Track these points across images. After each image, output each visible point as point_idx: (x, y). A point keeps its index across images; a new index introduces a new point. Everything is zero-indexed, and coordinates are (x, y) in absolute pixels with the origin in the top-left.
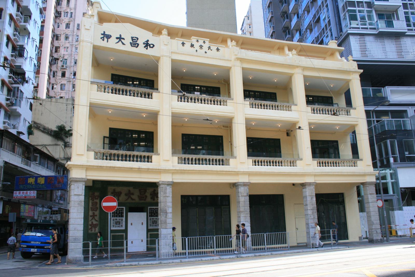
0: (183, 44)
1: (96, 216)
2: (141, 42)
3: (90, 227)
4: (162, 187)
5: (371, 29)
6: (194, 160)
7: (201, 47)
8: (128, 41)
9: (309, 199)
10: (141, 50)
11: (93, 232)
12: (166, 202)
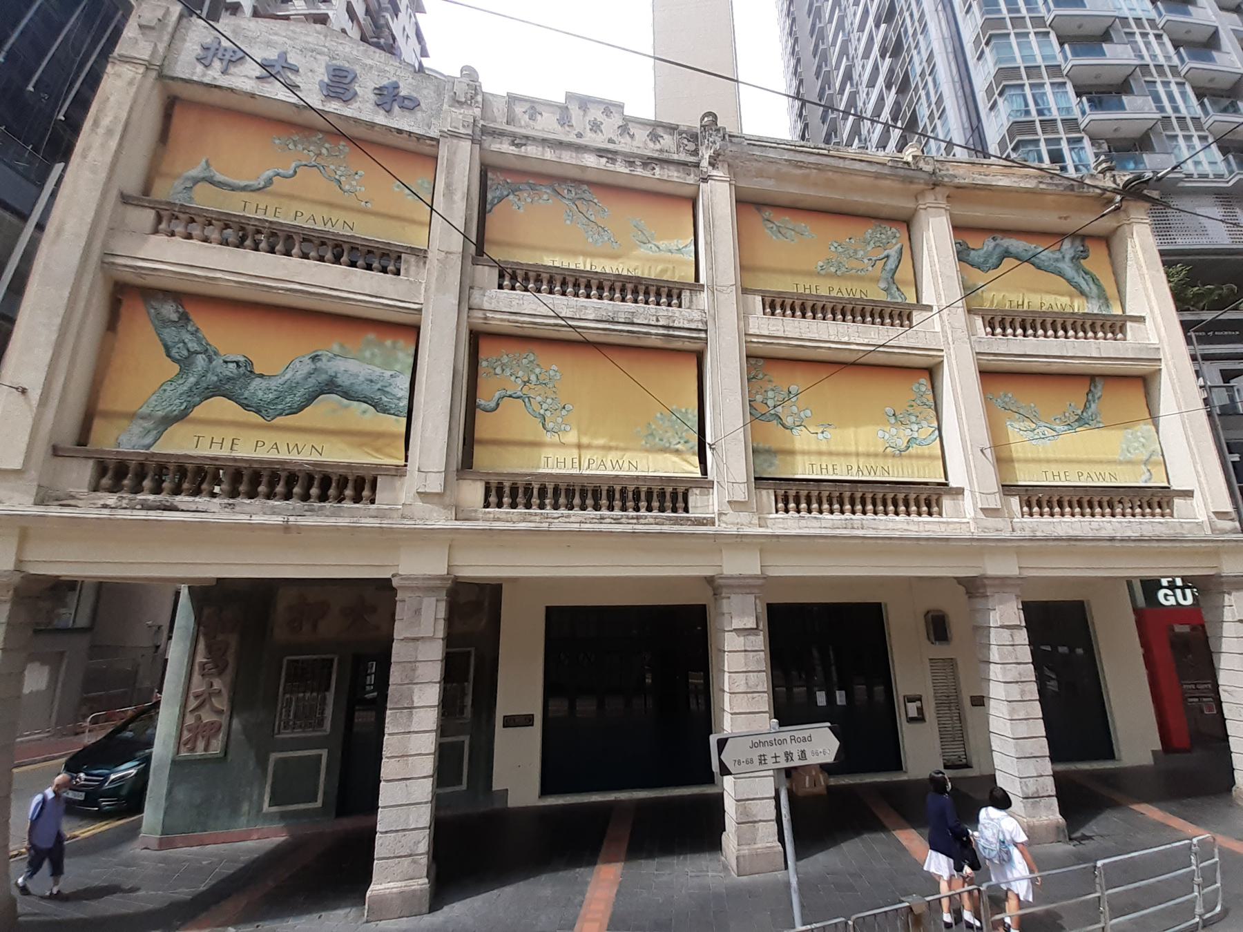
3: (186, 735)
6: (507, 490)
11: (200, 752)
12: (415, 662)
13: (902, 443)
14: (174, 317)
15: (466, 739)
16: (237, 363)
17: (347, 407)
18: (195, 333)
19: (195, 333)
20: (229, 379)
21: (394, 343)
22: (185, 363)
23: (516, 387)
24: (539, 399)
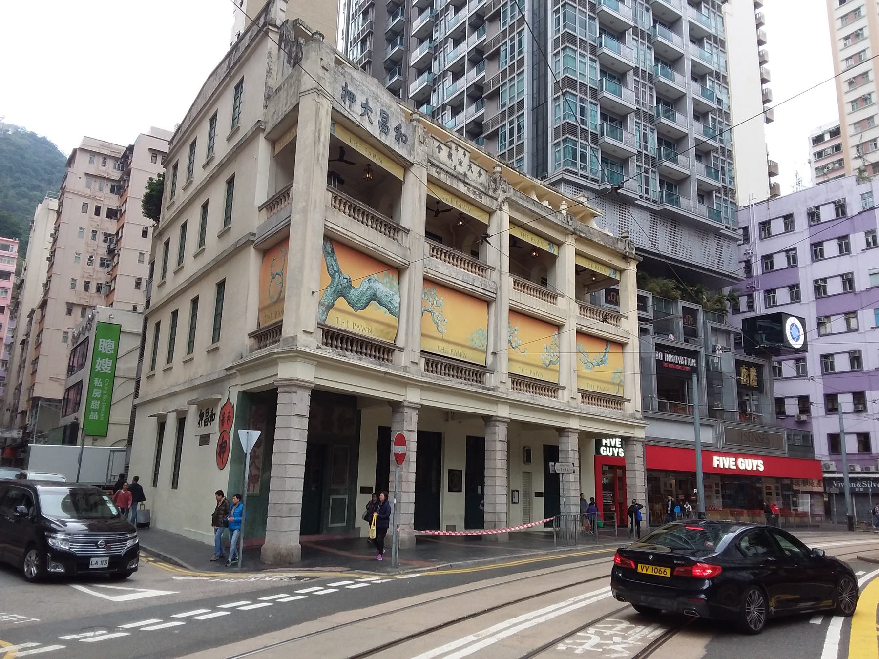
0: (440, 148)
1: (258, 457)
2: (392, 124)
4: (406, 413)
5: (593, 180)
7: (461, 163)
8: (376, 118)
9: (571, 453)
10: (389, 140)
13: (548, 362)
14: (330, 250)
15: (346, 497)
16: (347, 279)
17: (380, 308)
18: (335, 260)
19: (335, 260)
20: (345, 287)
21: (392, 276)
22: (332, 276)
23: (429, 307)
24: (437, 314)
